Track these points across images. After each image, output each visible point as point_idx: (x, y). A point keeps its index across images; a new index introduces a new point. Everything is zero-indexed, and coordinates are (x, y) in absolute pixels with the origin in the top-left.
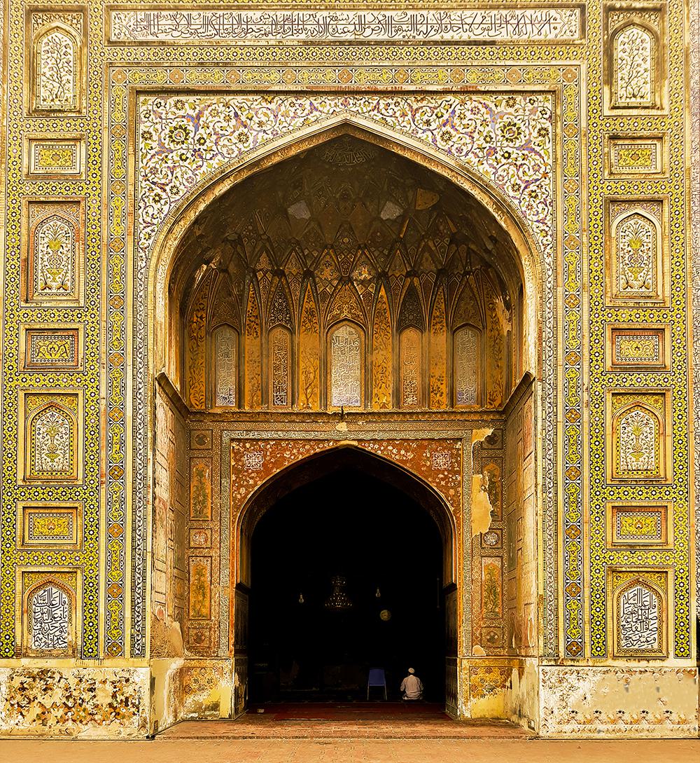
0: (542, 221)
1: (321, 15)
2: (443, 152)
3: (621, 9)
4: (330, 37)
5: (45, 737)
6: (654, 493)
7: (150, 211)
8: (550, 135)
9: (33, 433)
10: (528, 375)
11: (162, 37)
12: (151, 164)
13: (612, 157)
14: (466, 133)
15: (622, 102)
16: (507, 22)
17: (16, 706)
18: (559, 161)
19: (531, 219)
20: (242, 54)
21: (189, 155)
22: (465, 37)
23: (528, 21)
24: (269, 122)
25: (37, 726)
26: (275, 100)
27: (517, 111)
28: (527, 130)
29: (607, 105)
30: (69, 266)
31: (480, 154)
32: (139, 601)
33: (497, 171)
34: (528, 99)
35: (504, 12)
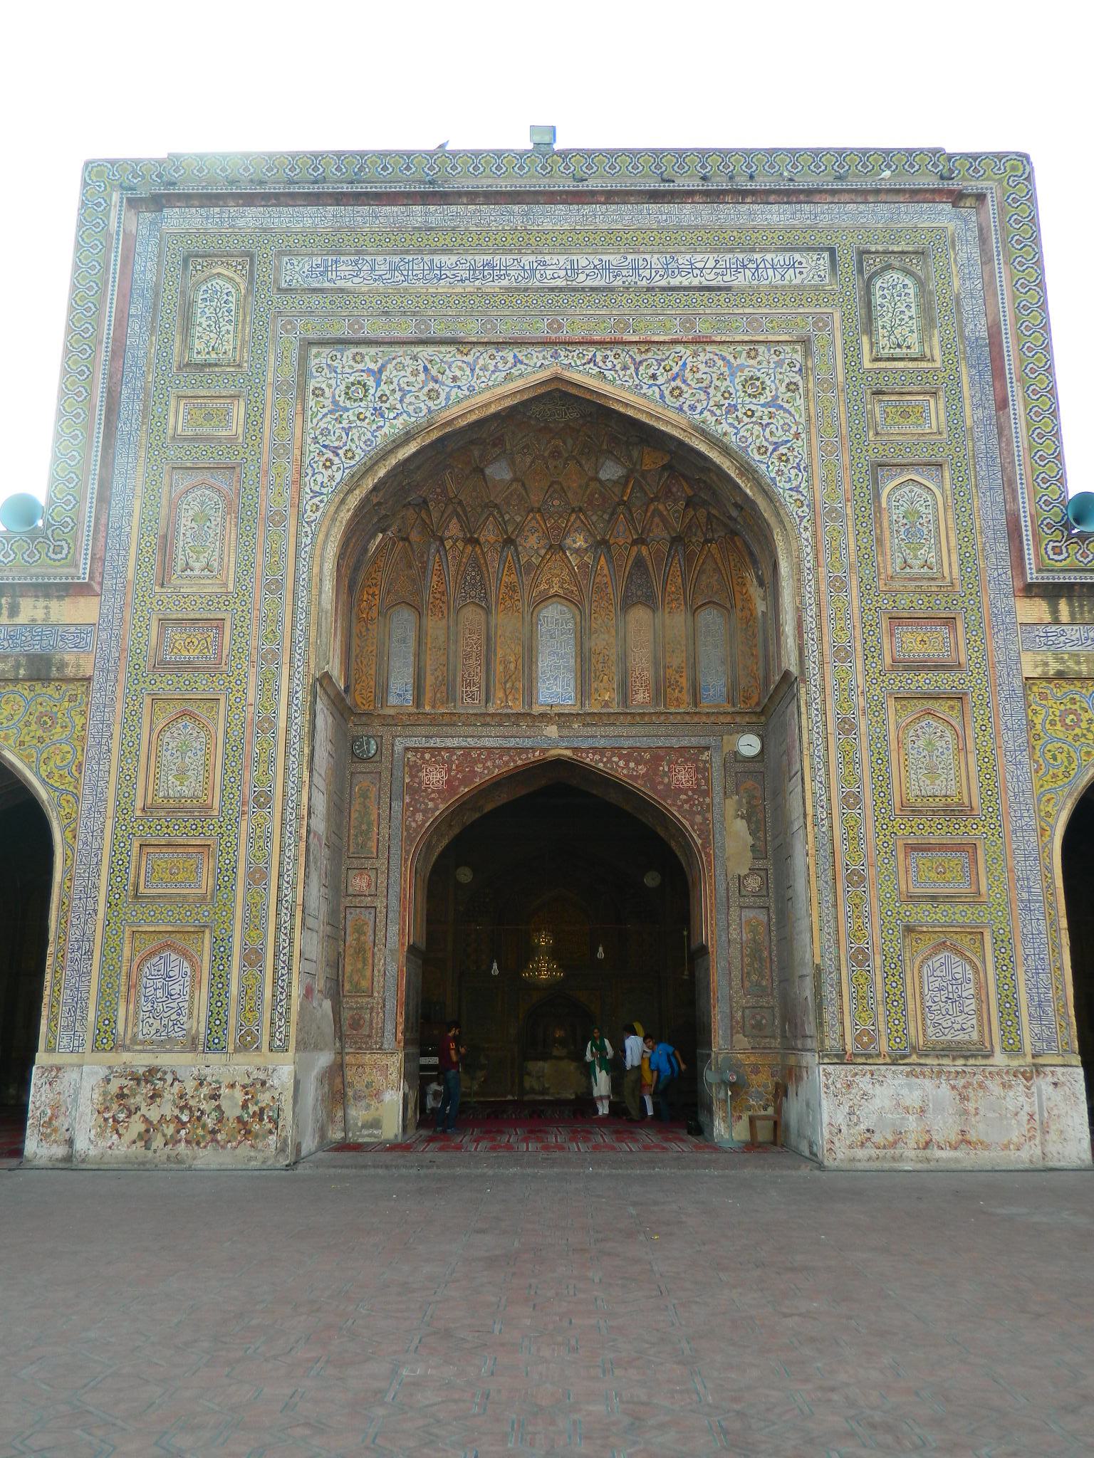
0: (796, 489)
1: (527, 260)
2: (673, 410)
3: (877, 252)
4: (538, 284)
5: (148, 1166)
6: (957, 826)
7: (319, 478)
8: (801, 390)
9: (159, 749)
10: (787, 674)
11: (340, 284)
12: (322, 425)
13: (878, 415)
14: (700, 388)
15: (886, 352)
16: (744, 267)
17: (111, 1120)
18: (813, 421)
19: (782, 486)
20: (433, 302)
21: (368, 414)
22: (696, 282)
23: (768, 266)
24: (465, 377)
25: (138, 1148)
26: (472, 352)
27: (759, 363)
28: (773, 384)
30: (218, 543)
31: (718, 412)
32: (284, 972)
33: (739, 431)
34: (772, 352)
35: (740, 256)
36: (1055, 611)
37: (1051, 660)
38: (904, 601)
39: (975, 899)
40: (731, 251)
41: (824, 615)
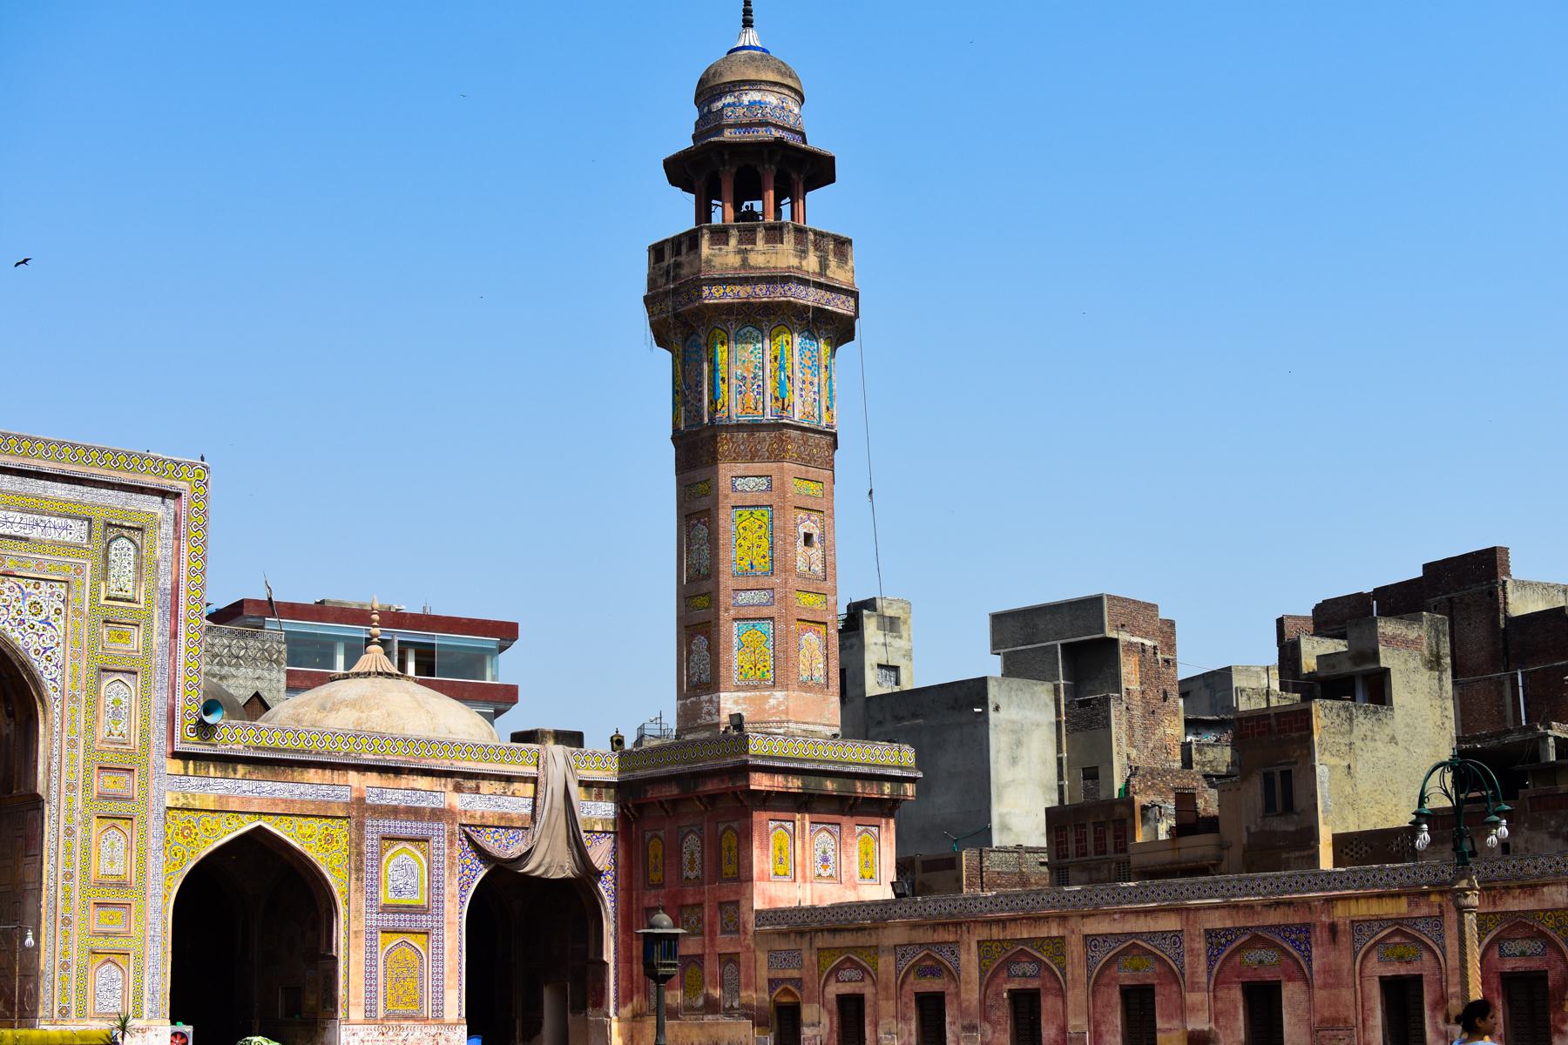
3: (116, 526)
14: (4, 606)
15: (113, 594)
16: (37, 525)
22: (7, 532)
27: (40, 593)
29: (103, 596)
35: (36, 517)
36: (186, 768)
37: (181, 798)
38: (107, 757)
39: (127, 935)
40: (32, 512)
41: (63, 762)
